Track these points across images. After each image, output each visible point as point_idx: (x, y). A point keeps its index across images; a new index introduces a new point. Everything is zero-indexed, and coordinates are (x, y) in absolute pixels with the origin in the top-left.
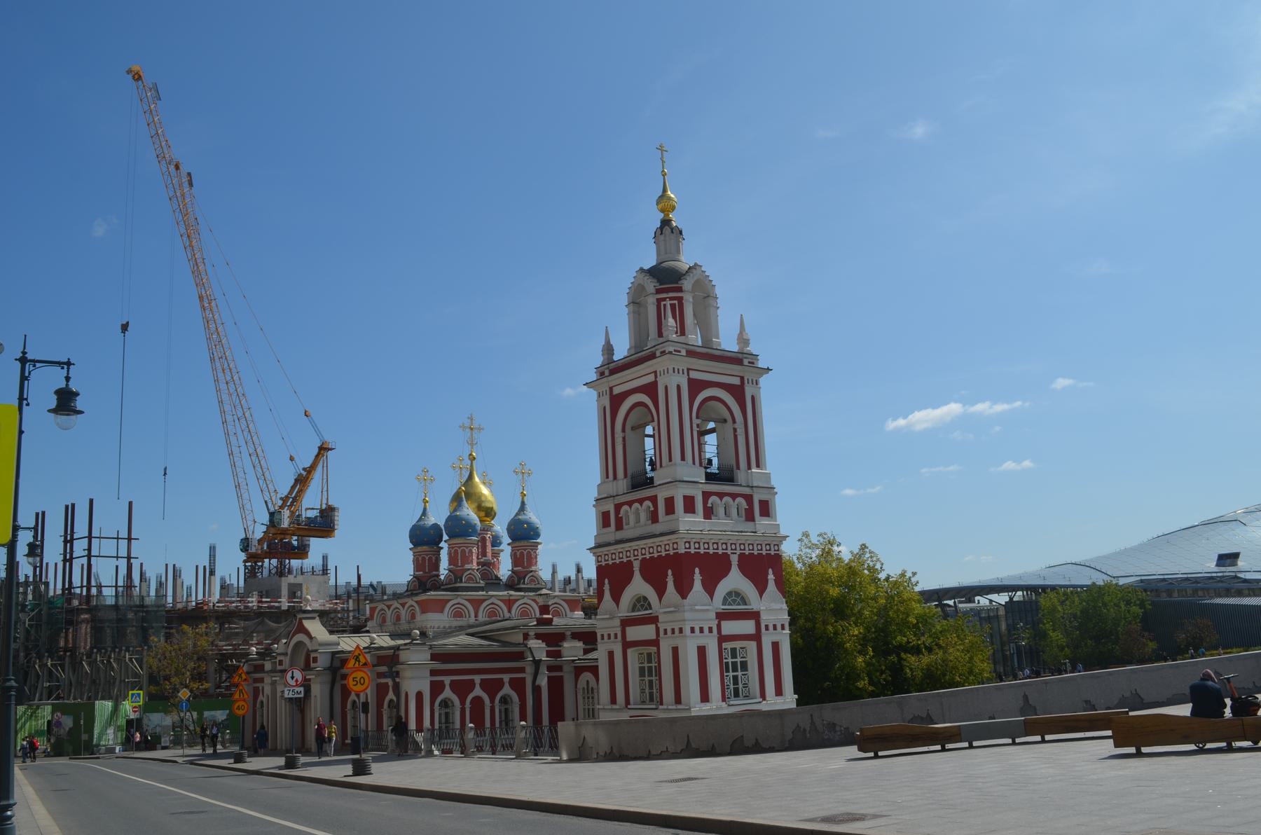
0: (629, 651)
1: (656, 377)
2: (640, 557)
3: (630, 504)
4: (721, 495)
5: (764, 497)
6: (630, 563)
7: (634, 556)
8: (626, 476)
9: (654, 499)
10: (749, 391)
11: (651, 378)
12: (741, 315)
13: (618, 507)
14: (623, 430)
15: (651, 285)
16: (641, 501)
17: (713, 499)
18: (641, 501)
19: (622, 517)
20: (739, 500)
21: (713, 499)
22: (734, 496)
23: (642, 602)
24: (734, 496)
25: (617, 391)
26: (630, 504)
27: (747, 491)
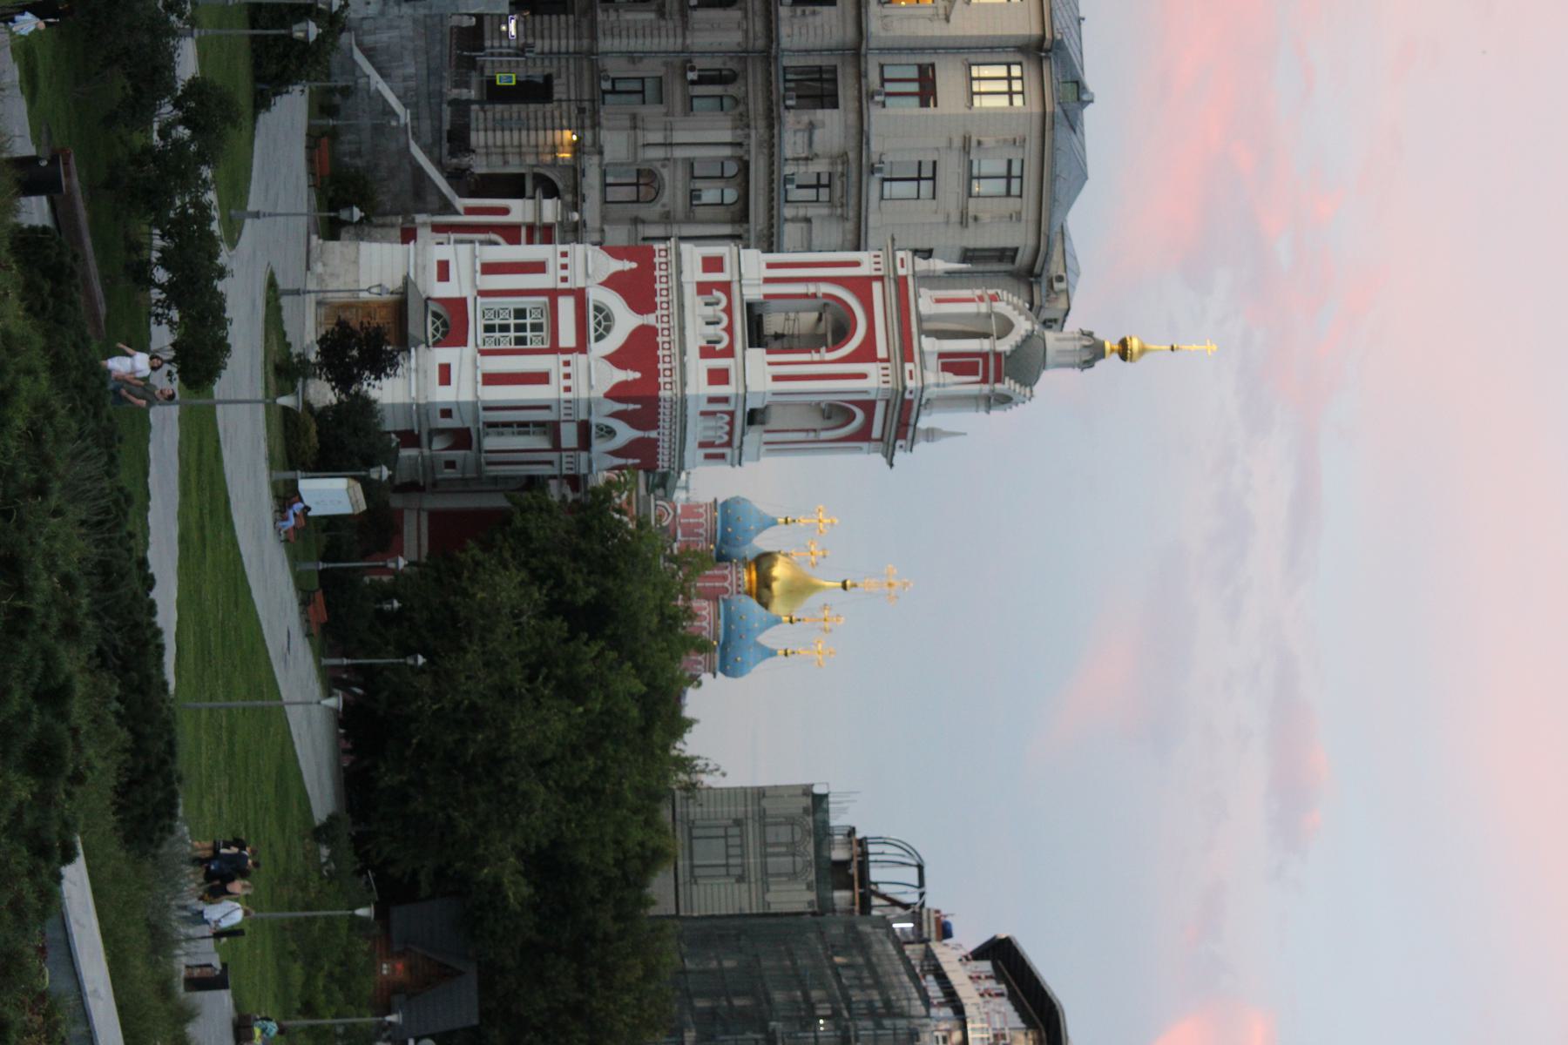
0: (545, 299)
1: (882, 361)
2: (659, 326)
3: (728, 310)
4: (731, 423)
5: (729, 457)
6: (651, 308)
7: (662, 316)
8: (767, 296)
9: (729, 352)
10: (865, 445)
11: (882, 352)
12: (965, 434)
13: (725, 287)
14: (826, 296)
15: (1005, 345)
16: (730, 330)
17: (727, 418)
18: (730, 330)
19: (711, 293)
20: (726, 438)
21: (727, 418)
22: (731, 433)
23: (606, 321)
24: (731, 433)
25: (877, 287)
26: (728, 310)
27: (736, 442)
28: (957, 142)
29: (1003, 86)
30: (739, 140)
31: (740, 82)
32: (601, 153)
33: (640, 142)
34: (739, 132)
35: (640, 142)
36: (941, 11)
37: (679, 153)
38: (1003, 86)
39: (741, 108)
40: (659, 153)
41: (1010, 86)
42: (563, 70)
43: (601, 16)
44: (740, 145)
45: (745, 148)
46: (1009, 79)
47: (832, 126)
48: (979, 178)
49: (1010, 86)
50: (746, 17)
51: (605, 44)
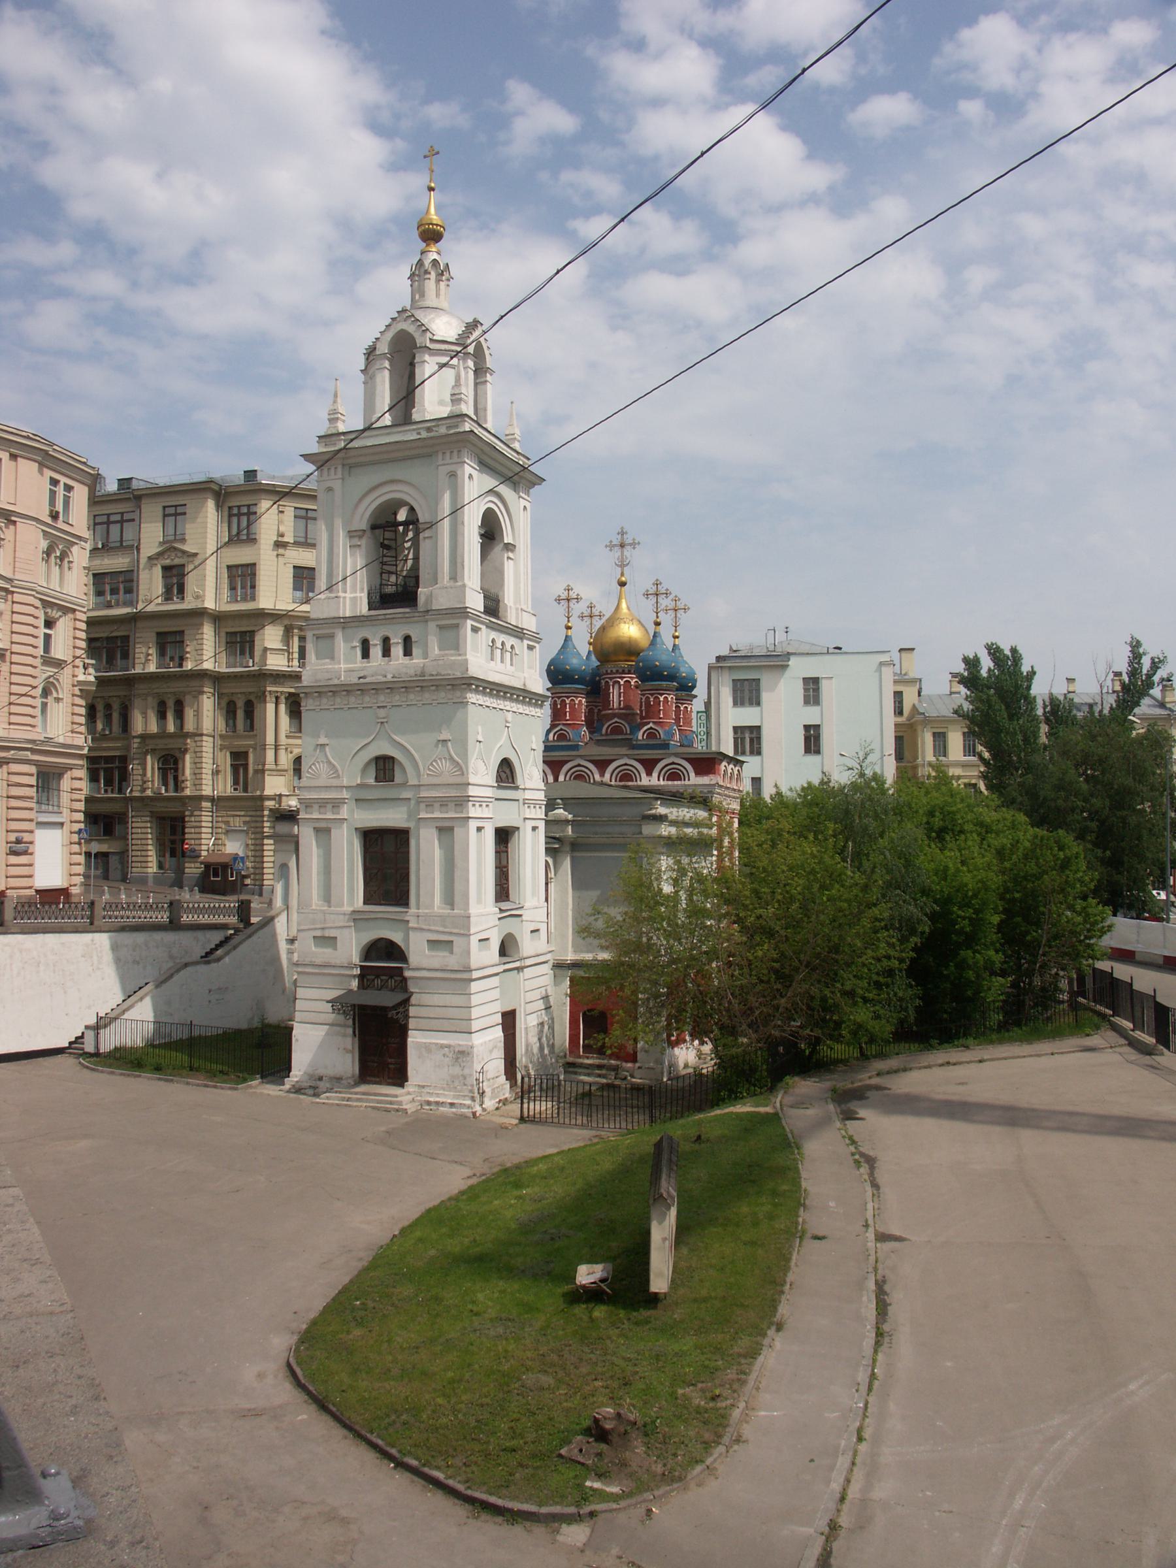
28: (281, 551)
29: (244, 520)
30: (274, 700)
31: (234, 698)
32: (280, 796)
33: (274, 767)
34: (268, 698)
35: (274, 767)
36: (191, 559)
37: (283, 740)
38: (244, 520)
39: (252, 698)
40: (282, 753)
41: (244, 514)
42: (225, 819)
43: (188, 792)
44: (277, 698)
45: (279, 694)
46: (239, 515)
47: (271, 637)
48: (306, 537)
49: (244, 514)
50: (189, 693)
51: (207, 791)
